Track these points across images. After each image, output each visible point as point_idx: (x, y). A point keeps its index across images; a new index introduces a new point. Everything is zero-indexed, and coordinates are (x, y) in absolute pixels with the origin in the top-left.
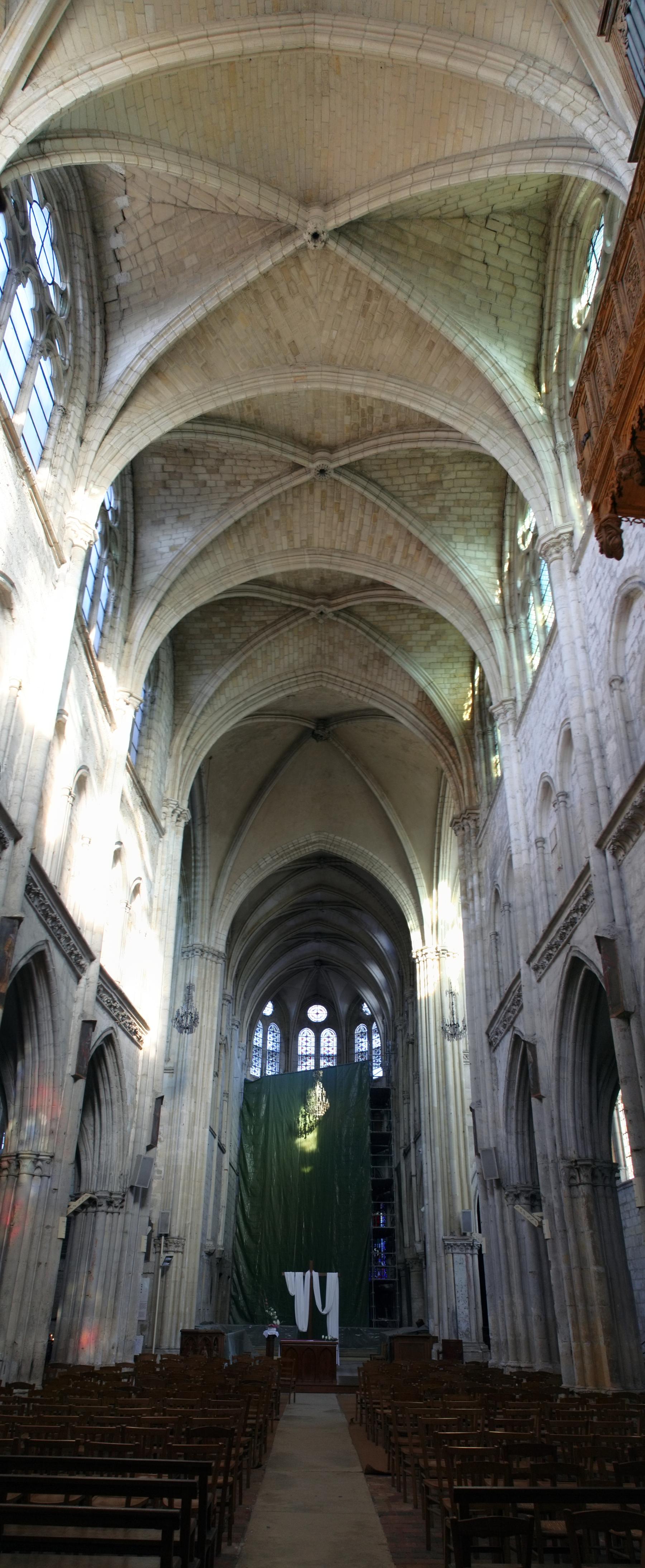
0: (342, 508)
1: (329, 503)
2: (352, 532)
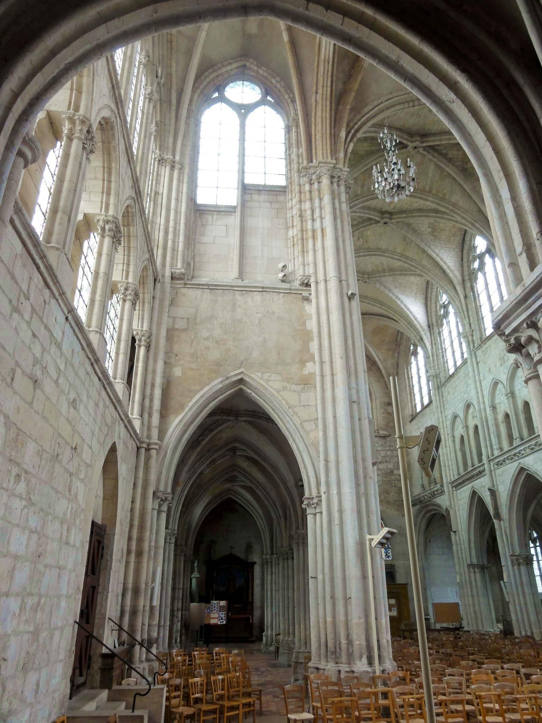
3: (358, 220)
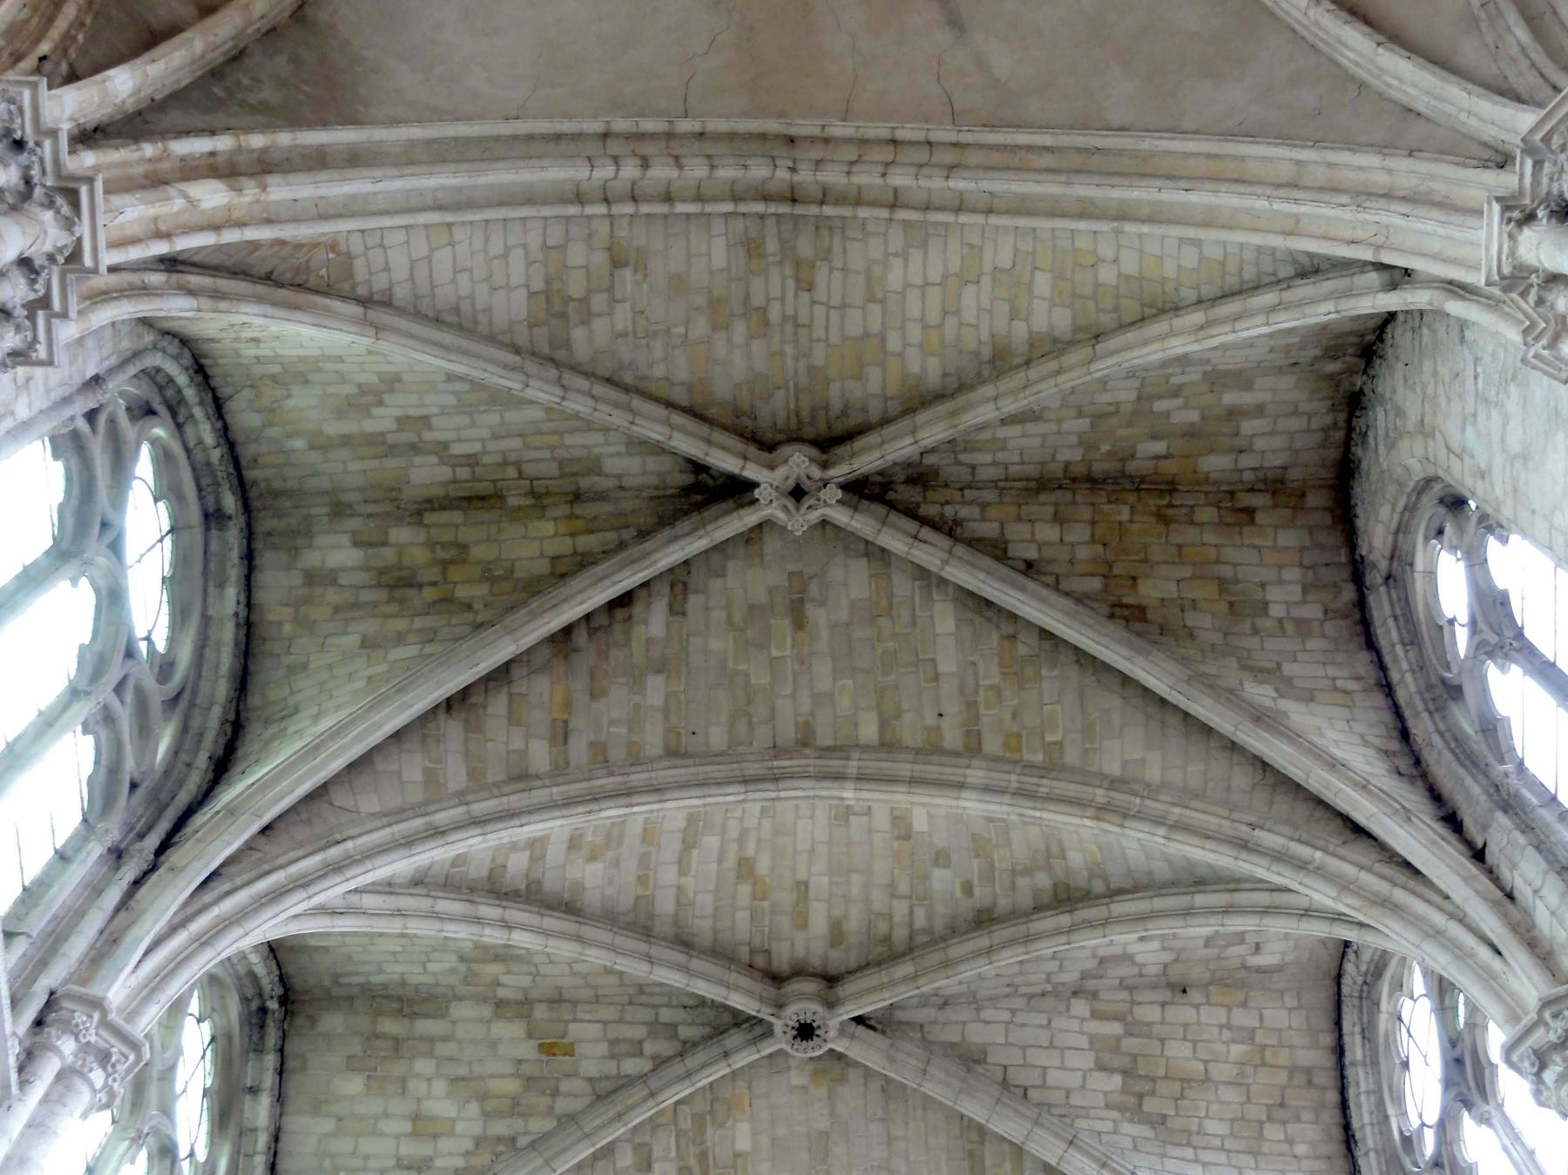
0: (745, 890)
1: (786, 898)
2: (712, 842)
3: (649, 1048)
